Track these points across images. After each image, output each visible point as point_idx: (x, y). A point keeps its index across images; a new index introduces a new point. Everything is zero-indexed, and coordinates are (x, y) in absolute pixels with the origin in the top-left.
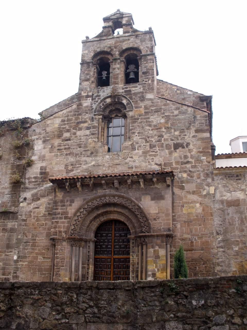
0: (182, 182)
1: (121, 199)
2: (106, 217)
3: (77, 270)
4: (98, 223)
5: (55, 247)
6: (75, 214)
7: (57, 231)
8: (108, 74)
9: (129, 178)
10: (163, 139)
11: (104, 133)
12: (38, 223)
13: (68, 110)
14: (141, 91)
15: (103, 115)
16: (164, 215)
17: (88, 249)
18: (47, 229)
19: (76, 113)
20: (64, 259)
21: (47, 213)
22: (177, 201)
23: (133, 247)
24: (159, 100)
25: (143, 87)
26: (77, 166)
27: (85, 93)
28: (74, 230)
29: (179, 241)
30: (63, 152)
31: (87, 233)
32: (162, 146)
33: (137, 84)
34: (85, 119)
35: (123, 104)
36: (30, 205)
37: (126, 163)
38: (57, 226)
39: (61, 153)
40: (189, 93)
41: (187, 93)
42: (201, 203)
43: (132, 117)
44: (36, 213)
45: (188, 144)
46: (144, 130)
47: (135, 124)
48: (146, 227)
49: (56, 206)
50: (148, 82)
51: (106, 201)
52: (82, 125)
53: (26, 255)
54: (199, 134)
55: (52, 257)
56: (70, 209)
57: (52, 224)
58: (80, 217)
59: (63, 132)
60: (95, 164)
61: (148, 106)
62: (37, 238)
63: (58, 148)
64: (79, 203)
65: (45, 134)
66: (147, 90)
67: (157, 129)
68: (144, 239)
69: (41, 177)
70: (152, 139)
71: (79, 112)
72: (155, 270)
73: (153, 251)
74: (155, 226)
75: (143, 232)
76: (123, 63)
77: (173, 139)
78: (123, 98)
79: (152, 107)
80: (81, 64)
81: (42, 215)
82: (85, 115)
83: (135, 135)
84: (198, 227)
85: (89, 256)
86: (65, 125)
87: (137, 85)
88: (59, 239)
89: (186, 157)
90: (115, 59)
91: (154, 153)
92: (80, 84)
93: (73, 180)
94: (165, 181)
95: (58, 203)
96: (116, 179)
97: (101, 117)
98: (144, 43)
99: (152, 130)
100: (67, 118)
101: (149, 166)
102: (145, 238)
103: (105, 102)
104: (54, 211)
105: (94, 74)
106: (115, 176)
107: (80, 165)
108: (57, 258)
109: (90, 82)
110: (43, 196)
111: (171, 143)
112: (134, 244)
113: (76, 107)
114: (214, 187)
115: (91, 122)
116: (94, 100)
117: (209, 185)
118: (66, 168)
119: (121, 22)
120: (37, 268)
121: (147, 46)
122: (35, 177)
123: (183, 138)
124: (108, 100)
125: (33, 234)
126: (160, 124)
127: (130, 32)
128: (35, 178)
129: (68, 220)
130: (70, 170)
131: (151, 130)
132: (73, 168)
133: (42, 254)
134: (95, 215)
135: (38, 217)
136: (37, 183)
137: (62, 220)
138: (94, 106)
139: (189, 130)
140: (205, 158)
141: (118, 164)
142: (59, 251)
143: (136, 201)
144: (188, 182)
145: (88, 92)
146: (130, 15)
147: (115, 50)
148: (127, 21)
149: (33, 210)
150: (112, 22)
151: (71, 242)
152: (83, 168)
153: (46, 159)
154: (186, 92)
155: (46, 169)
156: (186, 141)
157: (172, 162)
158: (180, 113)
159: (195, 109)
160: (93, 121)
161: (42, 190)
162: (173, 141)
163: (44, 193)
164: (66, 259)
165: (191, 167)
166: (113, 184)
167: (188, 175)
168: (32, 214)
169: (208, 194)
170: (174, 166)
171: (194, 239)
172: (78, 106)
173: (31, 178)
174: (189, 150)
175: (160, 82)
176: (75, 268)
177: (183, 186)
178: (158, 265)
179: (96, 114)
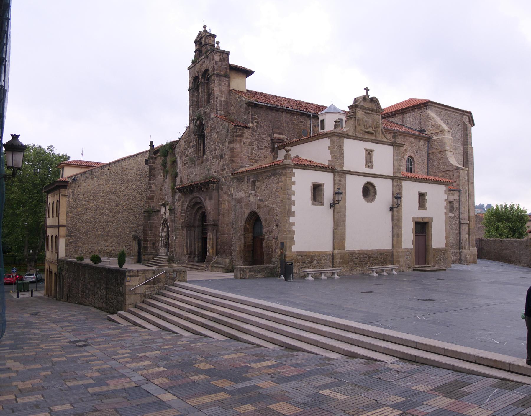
3: (191, 246)
15: (198, 135)
91: (213, 163)
174: (225, 159)
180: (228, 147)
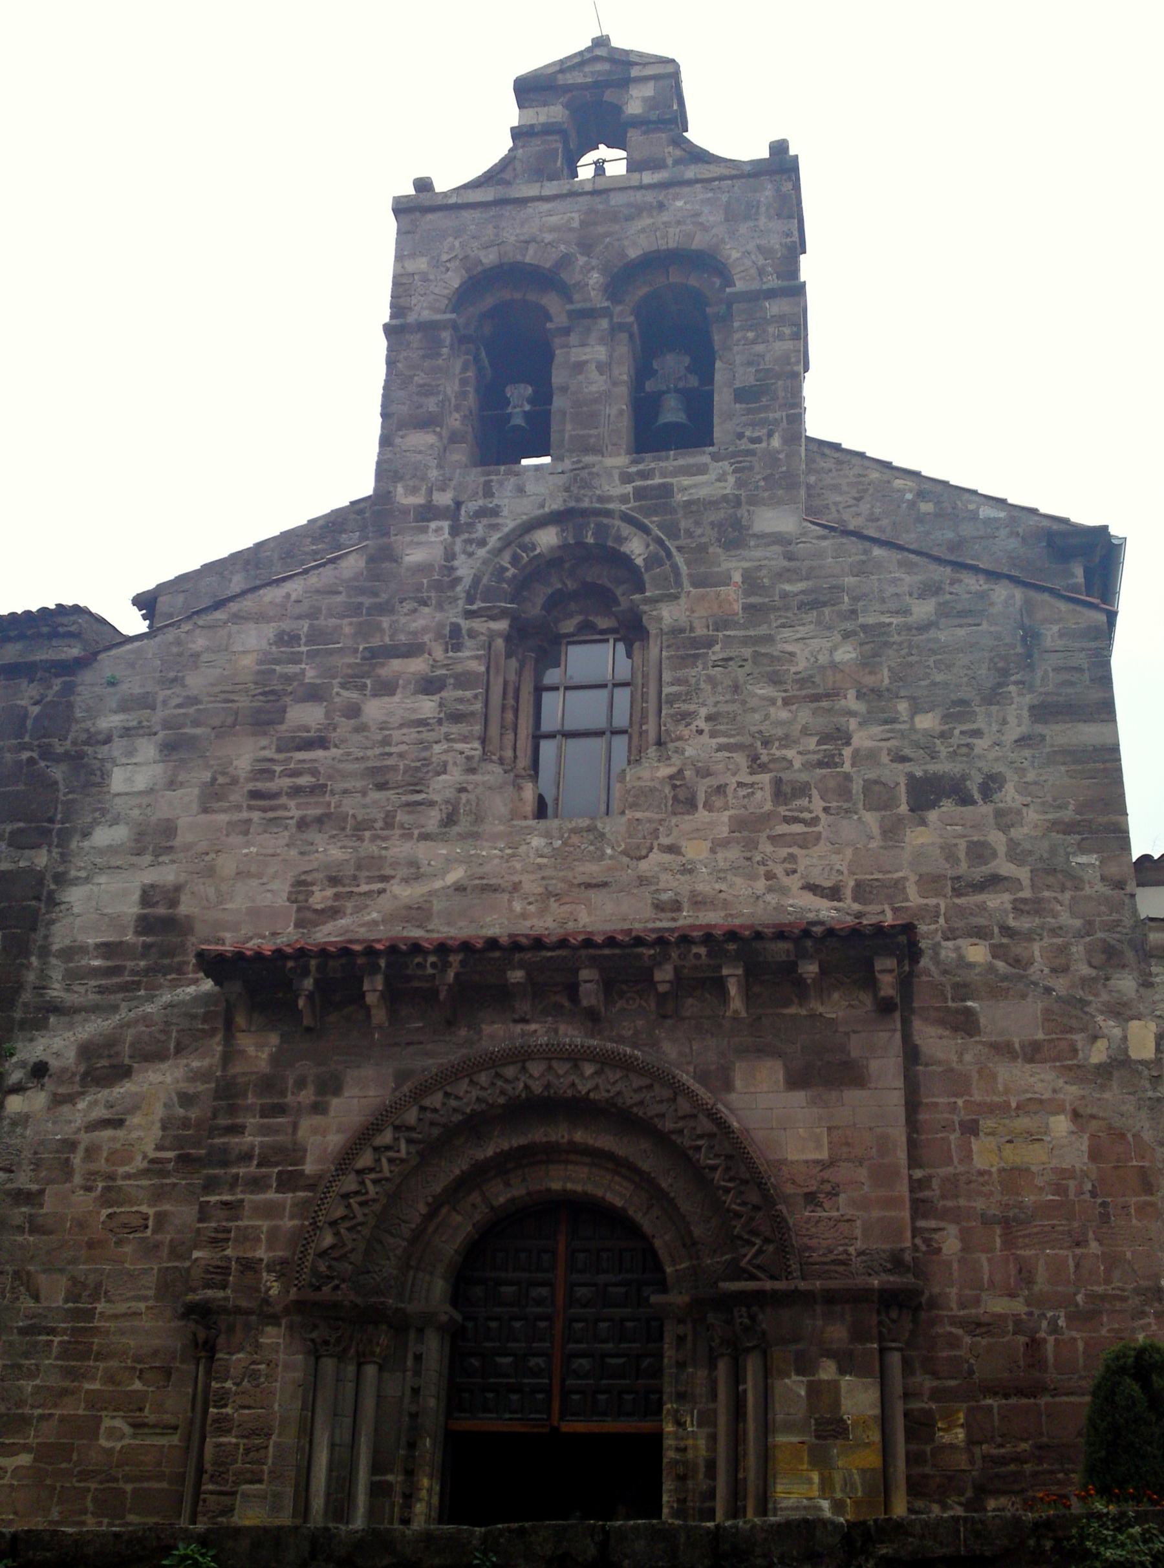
0: (963, 990)
1: (613, 1075)
2: (524, 1180)
4: (477, 1217)
5: (211, 1359)
6: (345, 1160)
7: (229, 1259)
8: (543, 396)
9: (666, 958)
10: (847, 752)
11: (516, 717)
12: (110, 1216)
13: (313, 580)
14: (727, 491)
15: (515, 618)
16: (863, 1174)
17: (409, 1374)
18: (165, 1252)
19: (360, 599)
20: (268, 1436)
21: (170, 1154)
22: (937, 1097)
23: (681, 1365)
24: (825, 543)
25: (734, 472)
26: (364, 888)
27: (414, 490)
28: (336, 1254)
29: (954, 1330)
30: (285, 808)
31: (411, 1273)
32: (844, 792)
33: (704, 453)
34: (415, 633)
35: (625, 561)
36: (66, 1109)
37: (642, 881)
38: (229, 1231)
39: (271, 815)
40: (985, 512)
41: (974, 517)
42: (1081, 1111)
43: (676, 631)
44: (105, 1154)
45: (991, 785)
46: (744, 702)
47: (693, 672)
48: (758, 1241)
49: (233, 1110)
50: (764, 445)
51: (526, 1087)
52: (396, 664)
53: (27, 1411)
54: (1057, 727)
55: (192, 1422)
56: (315, 1131)
57: (200, 1220)
58: (373, 1176)
59: (288, 699)
60: (465, 882)
61: (764, 572)
62: (100, 1306)
63: (251, 786)
64: (371, 1094)
65: (179, 706)
66: (757, 488)
67: (816, 698)
68: (753, 1318)
69: (147, 947)
70: (790, 753)
71: (376, 595)
72: (820, 1509)
73: (803, 1393)
74: (811, 1237)
75: (744, 1271)
76: (624, 336)
77: (907, 752)
78: (626, 530)
79: (789, 581)
80: (389, 330)
81: (139, 1164)
82: (415, 611)
83: (693, 727)
84: (1067, 1255)
85: (414, 1416)
86: (299, 662)
87: (705, 459)
88: (238, 1311)
89: (979, 852)
90: (590, 314)
91: (798, 828)
92: (386, 441)
93: (343, 961)
94: (870, 982)
95: (245, 1096)
96: (593, 959)
97: (502, 625)
98: (743, 228)
99: (787, 702)
100: (311, 626)
101: (768, 898)
102: (755, 1309)
103: (524, 548)
104: (218, 1141)
105: (463, 395)
106: (588, 943)
107: (380, 886)
108: (223, 1425)
109: (440, 435)
110: (153, 1055)
111: (896, 775)
112: (689, 1345)
113: (362, 564)
114: (1153, 1027)
115: (447, 651)
116: (466, 536)
117: (1121, 1011)
118: (301, 897)
119: (617, 109)
120: (88, 1490)
121: (763, 242)
122: (106, 945)
123: (964, 750)
124: (547, 539)
125: (74, 1280)
126: (829, 672)
127: (670, 162)
128: (108, 949)
129: (301, 1194)
130: (319, 907)
131: (779, 702)
132: (337, 896)
133: (131, 1405)
134: (459, 1166)
135: (111, 1177)
136: (116, 980)
137: (261, 1197)
138: (465, 569)
139: (998, 703)
140: (1093, 859)
141: (597, 886)
142: (237, 1384)
143: (701, 1091)
144: (997, 989)
145: (430, 492)
146: (670, 69)
147: (582, 260)
148: (652, 103)
149: (85, 1138)
150: (566, 106)
151: (315, 1327)
152: (395, 897)
153: (177, 842)
154: (971, 507)
155: (174, 903)
156: (981, 764)
157: (905, 879)
158: (947, 616)
159: (1032, 594)
160: (457, 648)
161: (146, 1019)
162: (907, 767)
163: (162, 1037)
164: (280, 1435)
165: (1009, 906)
166: (572, 990)
167: (997, 951)
168: (77, 1160)
169: (1120, 1062)
170: (914, 898)
171: (1044, 1324)
172: (371, 560)
173: (83, 950)
174: (999, 814)
175: (823, 455)
176: (328, 1495)
177: (968, 1012)
178: (838, 1477)
179: (474, 607)
180: (1023, 741)
